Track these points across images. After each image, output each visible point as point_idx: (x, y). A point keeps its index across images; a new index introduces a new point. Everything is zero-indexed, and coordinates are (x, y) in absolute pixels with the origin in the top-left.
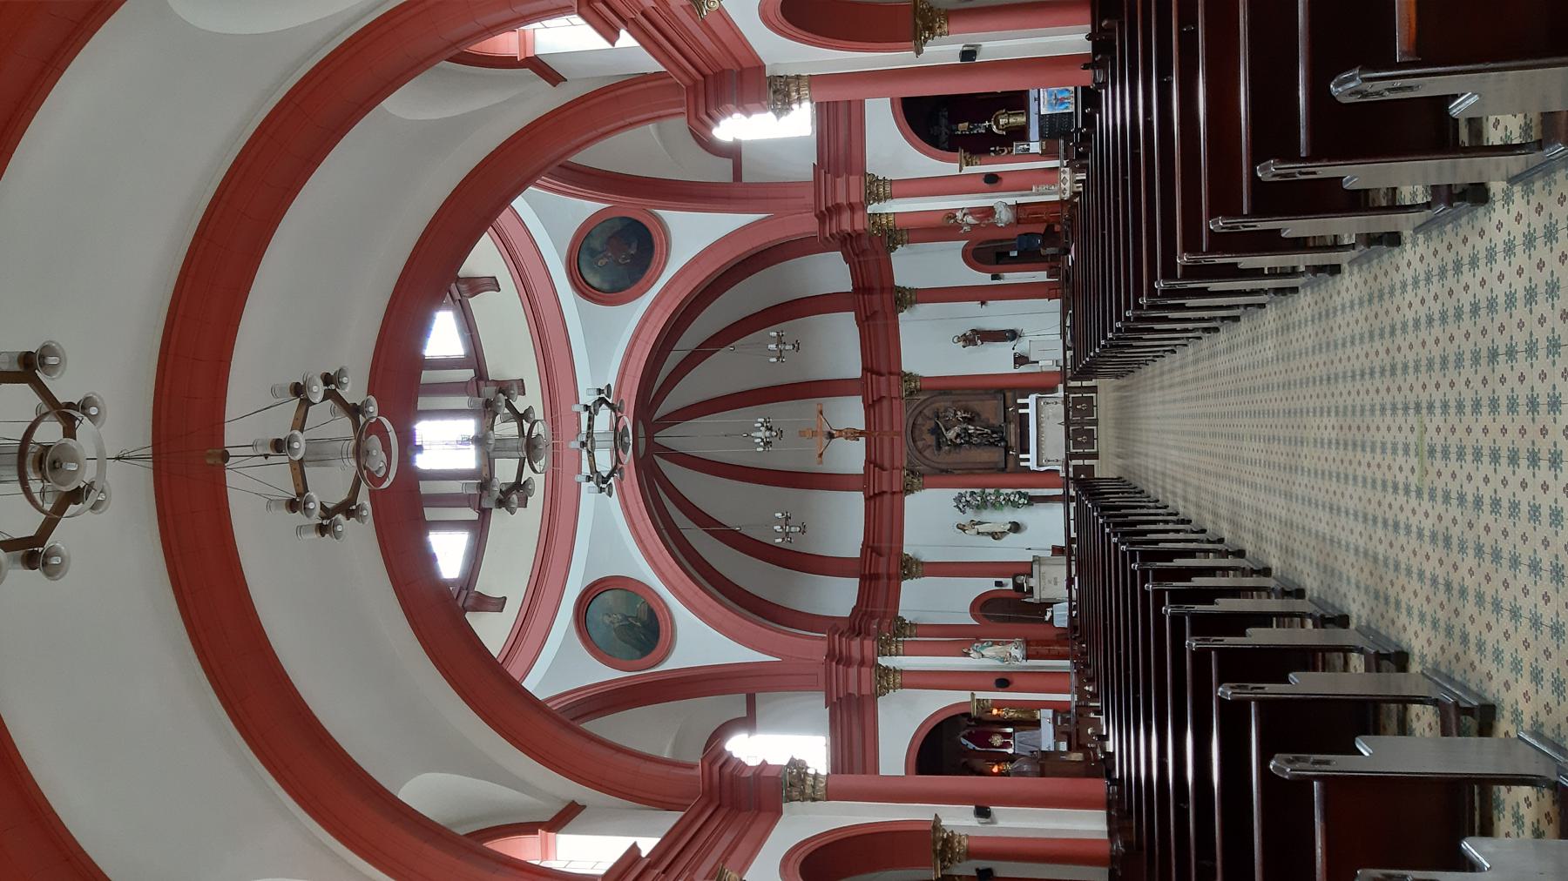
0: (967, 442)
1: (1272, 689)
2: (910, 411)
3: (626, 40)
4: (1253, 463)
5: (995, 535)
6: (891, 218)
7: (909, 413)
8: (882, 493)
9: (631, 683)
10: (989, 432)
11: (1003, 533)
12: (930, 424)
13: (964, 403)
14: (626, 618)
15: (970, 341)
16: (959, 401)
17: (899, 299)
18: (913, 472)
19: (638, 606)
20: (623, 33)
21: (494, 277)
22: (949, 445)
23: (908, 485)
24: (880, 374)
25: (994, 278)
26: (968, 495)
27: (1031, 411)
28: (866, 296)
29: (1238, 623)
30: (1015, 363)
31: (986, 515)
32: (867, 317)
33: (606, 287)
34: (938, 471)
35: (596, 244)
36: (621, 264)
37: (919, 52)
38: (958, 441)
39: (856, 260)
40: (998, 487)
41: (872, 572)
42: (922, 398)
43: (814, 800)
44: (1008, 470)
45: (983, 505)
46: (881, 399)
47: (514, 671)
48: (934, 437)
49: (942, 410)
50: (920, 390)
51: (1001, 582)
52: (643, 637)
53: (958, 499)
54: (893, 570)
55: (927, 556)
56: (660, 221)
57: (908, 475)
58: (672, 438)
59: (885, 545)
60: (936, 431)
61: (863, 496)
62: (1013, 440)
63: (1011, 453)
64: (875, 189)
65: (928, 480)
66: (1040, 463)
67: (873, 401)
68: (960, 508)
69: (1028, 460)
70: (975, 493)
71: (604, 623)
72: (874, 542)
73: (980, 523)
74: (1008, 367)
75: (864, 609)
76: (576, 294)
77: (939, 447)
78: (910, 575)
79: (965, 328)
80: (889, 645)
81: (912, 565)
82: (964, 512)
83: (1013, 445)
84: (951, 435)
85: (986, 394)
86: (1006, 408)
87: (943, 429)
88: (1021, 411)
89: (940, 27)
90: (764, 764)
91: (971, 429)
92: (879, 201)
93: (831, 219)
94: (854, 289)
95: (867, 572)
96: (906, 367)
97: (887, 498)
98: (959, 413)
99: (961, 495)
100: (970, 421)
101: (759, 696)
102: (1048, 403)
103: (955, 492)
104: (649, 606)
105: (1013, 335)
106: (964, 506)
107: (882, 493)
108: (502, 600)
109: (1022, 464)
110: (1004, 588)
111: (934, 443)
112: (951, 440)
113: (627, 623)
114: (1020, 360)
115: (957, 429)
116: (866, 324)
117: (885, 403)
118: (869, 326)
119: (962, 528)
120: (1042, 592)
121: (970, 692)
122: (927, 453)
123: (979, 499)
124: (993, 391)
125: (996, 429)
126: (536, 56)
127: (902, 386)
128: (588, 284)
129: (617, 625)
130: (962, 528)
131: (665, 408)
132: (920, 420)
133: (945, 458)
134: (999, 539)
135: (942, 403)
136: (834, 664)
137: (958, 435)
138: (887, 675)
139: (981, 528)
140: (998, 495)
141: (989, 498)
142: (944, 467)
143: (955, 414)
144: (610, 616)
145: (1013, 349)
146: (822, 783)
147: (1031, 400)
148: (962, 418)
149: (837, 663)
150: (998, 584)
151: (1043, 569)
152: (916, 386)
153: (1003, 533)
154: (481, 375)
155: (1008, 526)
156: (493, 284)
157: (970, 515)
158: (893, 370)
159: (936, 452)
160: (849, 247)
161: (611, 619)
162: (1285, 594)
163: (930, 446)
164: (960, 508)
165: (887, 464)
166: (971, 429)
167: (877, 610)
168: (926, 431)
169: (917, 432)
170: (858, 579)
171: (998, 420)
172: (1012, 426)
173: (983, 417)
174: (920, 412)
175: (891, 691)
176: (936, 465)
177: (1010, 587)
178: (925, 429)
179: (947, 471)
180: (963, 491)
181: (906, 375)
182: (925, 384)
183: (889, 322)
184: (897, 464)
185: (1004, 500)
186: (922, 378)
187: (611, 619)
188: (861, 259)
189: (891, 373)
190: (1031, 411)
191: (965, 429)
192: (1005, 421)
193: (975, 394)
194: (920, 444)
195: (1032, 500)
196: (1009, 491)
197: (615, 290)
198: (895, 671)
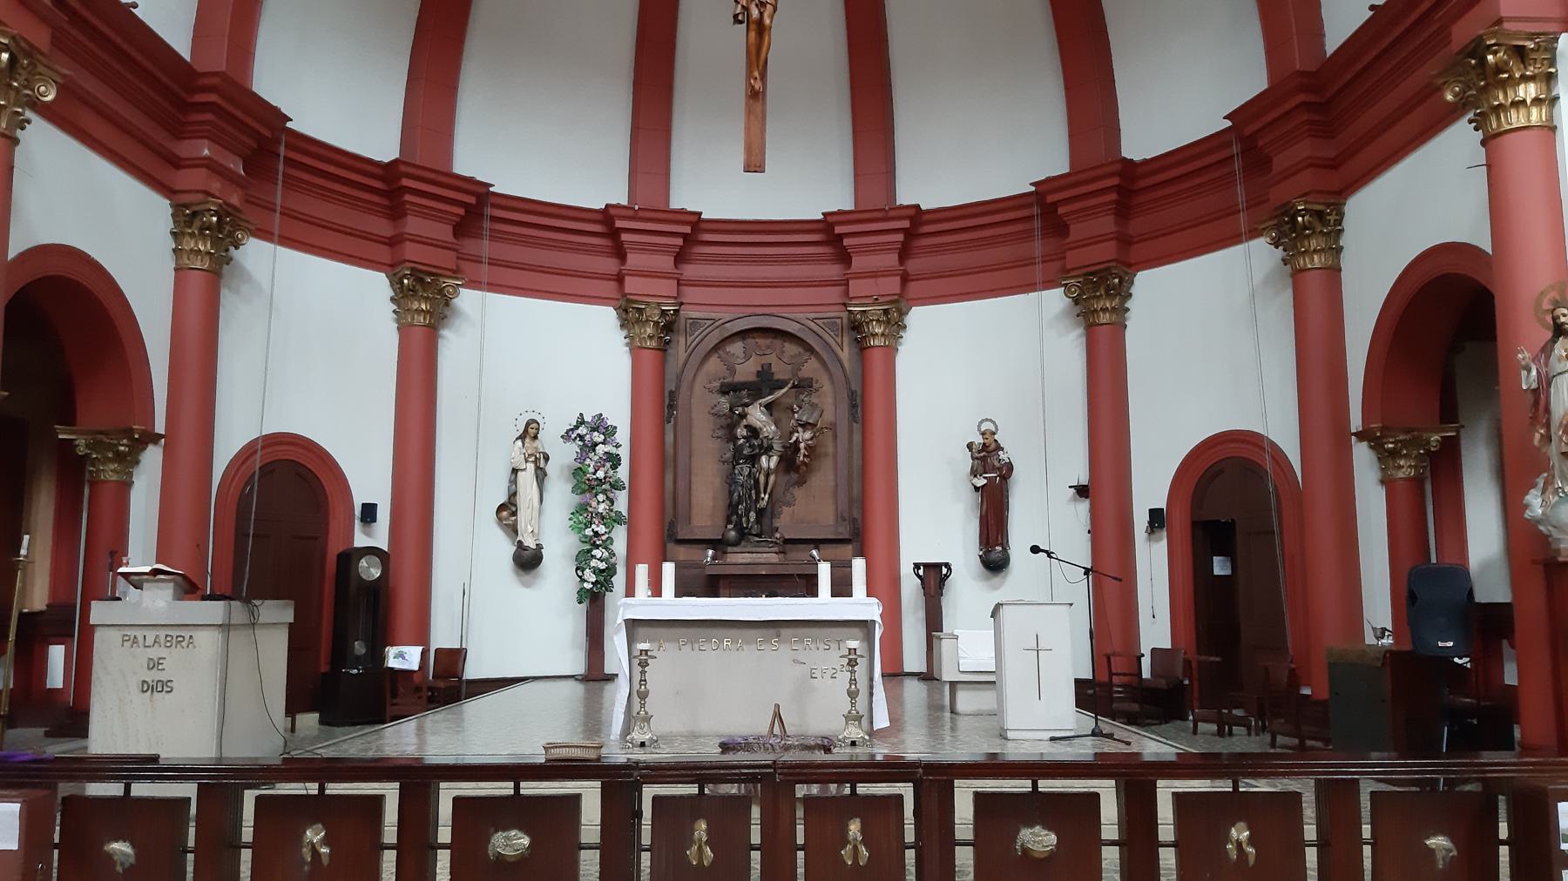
0: (738, 451)
2: (812, 325)
5: (508, 509)
6: (1536, 116)
7: (812, 325)
8: (620, 253)
10: (763, 504)
11: (513, 530)
12: (780, 371)
13: (830, 450)
15: (983, 459)
16: (835, 437)
17: (1103, 279)
18: (669, 328)
22: (731, 410)
23: (640, 311)
24: (904, 253)
25: (1156, 518)
26: (608, 448)
27: (823, 605)
28: (1113, 196)
30: (927, 566)
31: (561, 495)
32: (1055, 204)
34: (670, 386)
38: (741, 432)
40: (632, 524)
41: (408, 197)
42: (846, 354)
44: (671, 546)
45: (585, 484)
46: (844, 258)
48: (752, 378)
49: (815, 400)
50: (862, 347)
51: (374, 520)
53: (599, 425)
54: (411, 251)
55: (454, 349)
59: (485, 247)
60: (763, 384)
62: (741, 559)
63: (710, 552)
65: (649, 357)
66: (641, 631)
67: (841, 237)
68: (577, 427)
69: (656, 590)
70: (614, 467)
72: (494, 219)
73: (541, 475)
74: (915, 546)
77: (725, 390)
78: (402, 296)
79: (1012, 450)
81: (427, 299)
82: (566, 437)
83: (731, 558)
84: (757, 415)
85: (851, 500)
86: (817, 543)
87: (769, 398)
88: (824, 571)
91: (769, 462)
94: (1130, 168)
95: (405, 182)
96: (921, 318)
97: (610, 265)
98: (808, 435)
99: (609, 432)
100: (789, 461)
102: (852, 663)
103: (620, 417)
105: (994, 562)
106: (581, 437)
107: (620, 253)
109: (642, 571)
110: (357, 523)
111: (739, 378)
112: (743, 416)
114: (934, 577)
115: (769, 429)
116: (1035, 210)
117: (833, 271)
118: (1029, 218)
119: (530, 432)
120: (115, 635)
122: (714, 364)
123: (600, 474)
124: (856, 515)
125: (766, 521)
127: (873, 304)
130: (530, 432)
132: (791, 349)
133: (703, 405)
134: (500, 519)
135: (828, 403)
137: (754, 432)
140: (612, 519)
141: (601, 497)
142: (681, 400)
143: (805, 426)
145: (1035, 550)
147: (862, 605)
148: (797, 441)
150: (369, 512)
151: (207, 642)
152: (874, 335)
153: (513, 530)
155: (530, 542)
157: (563, 455)
158: (912, 286)
159: (717, 384)
160: (1301, 98)
163: (733, 371)
164: (577, 427)
165: (690, 271)
166: (769, 462)
167: (280, 183)
168: (766, 360)
169: (762, 342)
171: (787, 523)
172: (774, 558)
173: (798, 492)
174: (809, 349)
176: (685, 385)
177: (360, 540)
178: (772, 359)
179: (671, 407)
180: (623, 436)
181: (902, 313)
182: (876, 358)
183: (1038, 268)
184: (691, 294)
185: (596, 534)
186: (891, 352)
189: (905, 279)
190: (823, 605)
191: (770, 448)
192: (787, 541)
193: (850, 476)
194: (737, 348)
195: (594, 600)
196: (620, 545)
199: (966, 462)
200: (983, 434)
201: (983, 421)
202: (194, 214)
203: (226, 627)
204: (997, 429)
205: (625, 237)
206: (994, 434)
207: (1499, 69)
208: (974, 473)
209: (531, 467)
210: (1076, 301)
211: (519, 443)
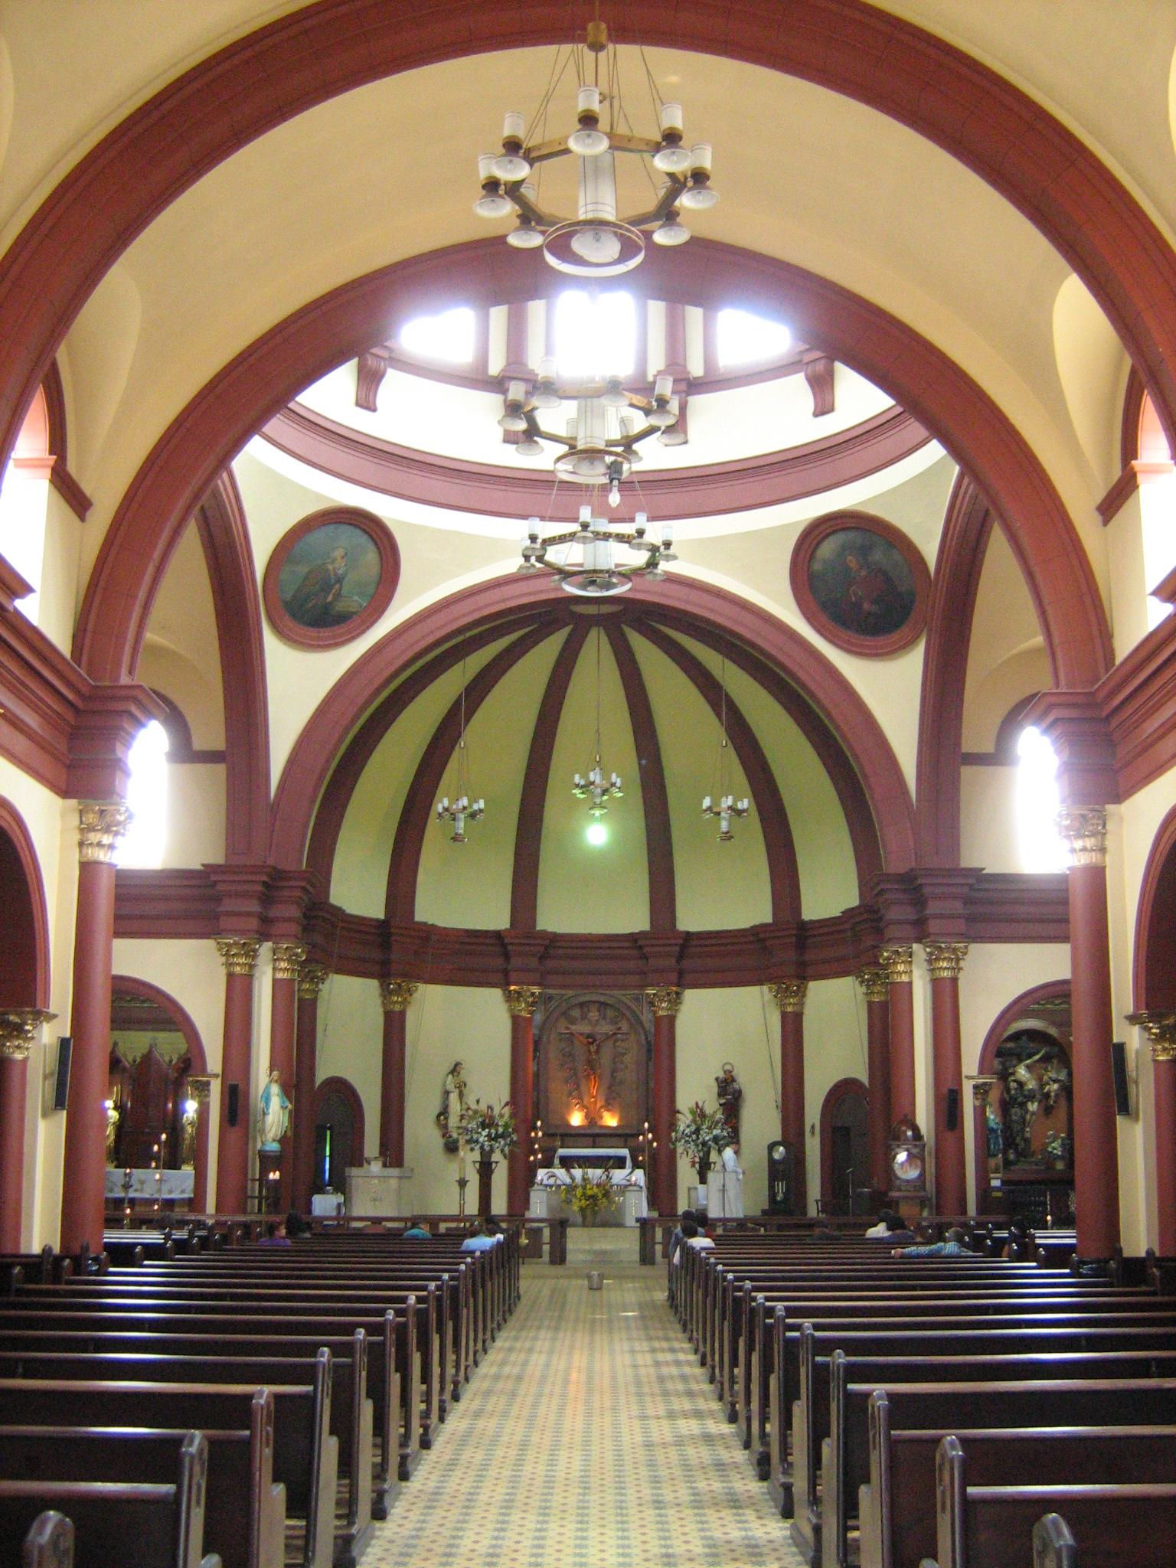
1: (264, 1456)
2: (624, 999)
3: (1156, 613)
4: (552, 1462)
8: (507, 957)
9: (248, 587)
14: (339, 580)
17: (787, 988)
18: (533, 1004)
19: (356, 598)
20: (1167, 609)
21: (832, 410)
24: (681, 957)
29: (345, 1427)
33: (817, 566)
35: (877, 556)
36: (848, 589)
37: (1133, 1019)
39: (847, 926)
43: (81, 844)
46: (645, 957)
47: (276, 425)
52: (310, 605)
56: (906, 645)
57: (533, 994)
58: (596, 652)
61: (503, 928)
64: (946, 955)
67: (641, 947)
71: (334, 549)
75: (341, 924)
76: (806, 523)
78: (386, 993)
79: (743, 1081)
80: (289, 960)
89: (1164, 1049)
90: (127, 773)
92: (929, 962)
93: (904, 891)
97: (499, 962)
101: (221, 769)
104: (355, 613)
107: (507, 957)
108: (373, 407)
113: (333, 581)
121: (221, 1073)
126: (1136, 487)
128: (818, 544)
129: (330, 567)
131: (641, 645)
136: (265, 878)
138: (247, 955)
139: (454, 1097)
144: (343, 557)
146: (105, 856)
149: (265, 883)
151: (394, 1182)
154: (692, 386)
156: (824, 407)
160: (866, 916)
161: (339, 560)
162: (404, 1459)
165: (550, 964)
170: (381, 916)
175: (224, 959)
186: (671, 1020)
187: (339, 560)
188: (849, 934)
189: (681, 973)
197: (812, 578)
198: (252, 967)
199: (715, 1090)
200: (725, 1072)
201: (726, 1064)
202: (309, 971)
203: (400, 1178)
204: (733, 1067)
205: (510, 948)
206: (731, 1072)
207: (888, 958)
208: (720, 1095)
209: (457, 1091)
210: (775, 996)
211: (450, 1076)
